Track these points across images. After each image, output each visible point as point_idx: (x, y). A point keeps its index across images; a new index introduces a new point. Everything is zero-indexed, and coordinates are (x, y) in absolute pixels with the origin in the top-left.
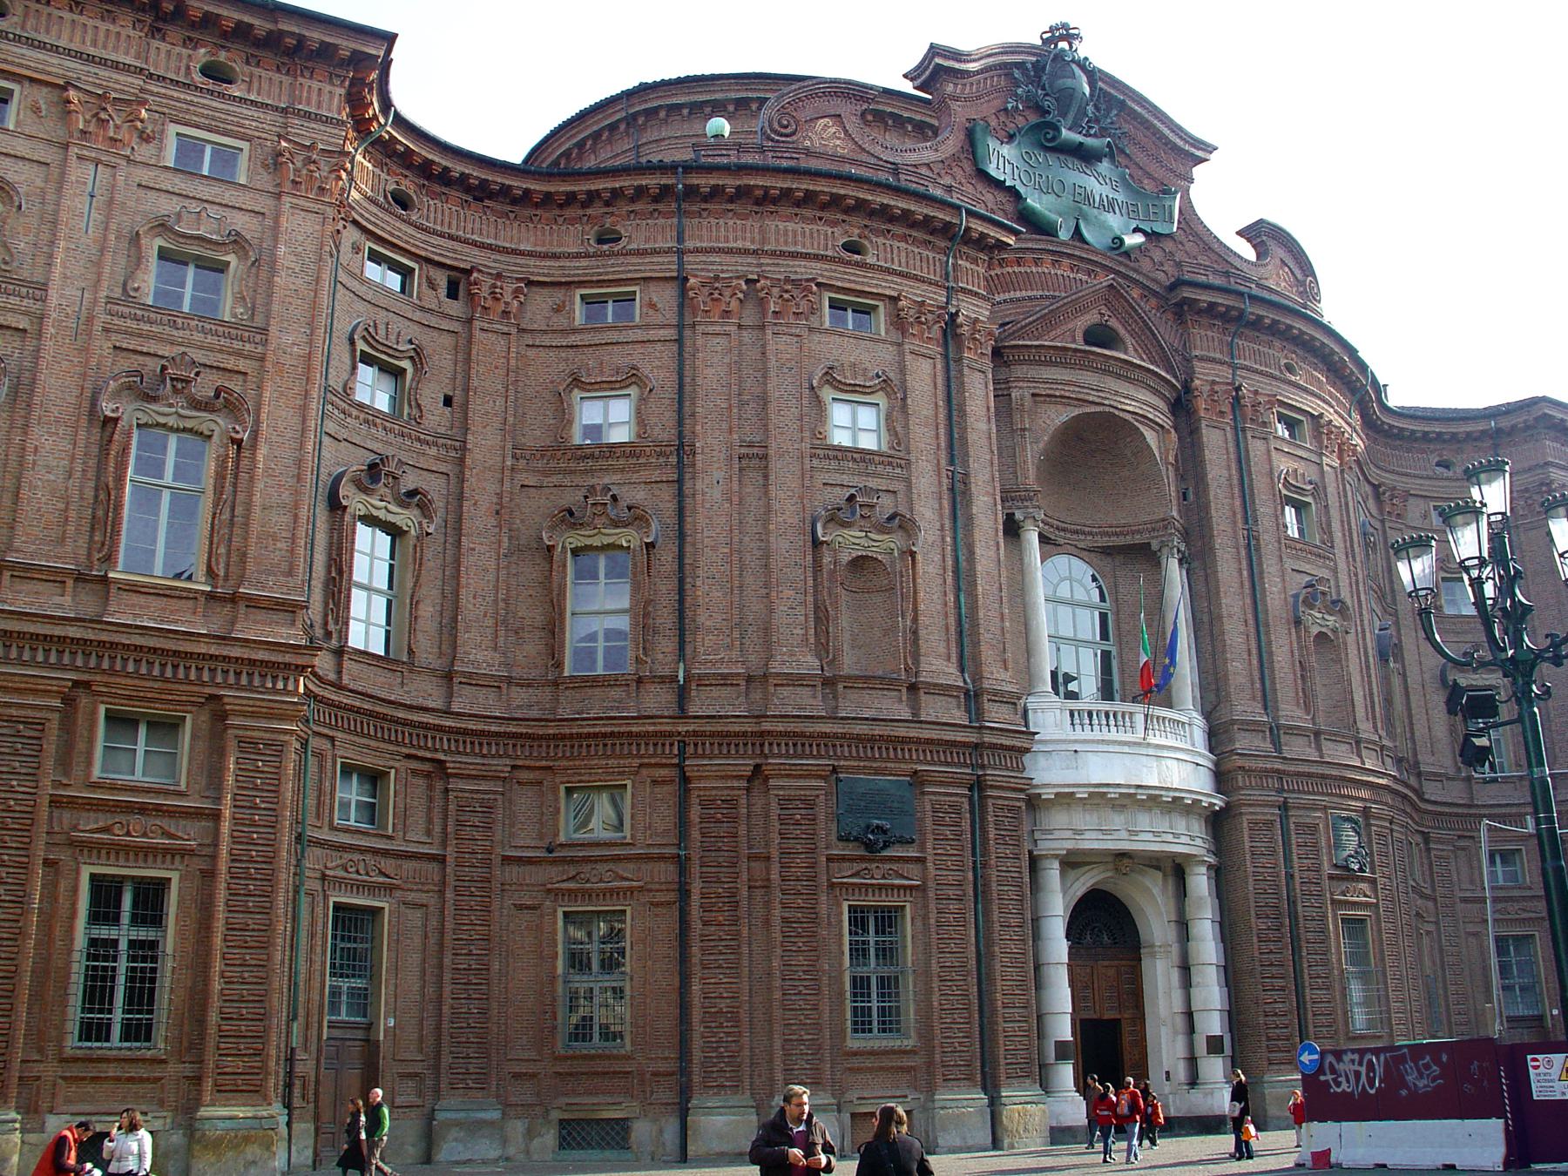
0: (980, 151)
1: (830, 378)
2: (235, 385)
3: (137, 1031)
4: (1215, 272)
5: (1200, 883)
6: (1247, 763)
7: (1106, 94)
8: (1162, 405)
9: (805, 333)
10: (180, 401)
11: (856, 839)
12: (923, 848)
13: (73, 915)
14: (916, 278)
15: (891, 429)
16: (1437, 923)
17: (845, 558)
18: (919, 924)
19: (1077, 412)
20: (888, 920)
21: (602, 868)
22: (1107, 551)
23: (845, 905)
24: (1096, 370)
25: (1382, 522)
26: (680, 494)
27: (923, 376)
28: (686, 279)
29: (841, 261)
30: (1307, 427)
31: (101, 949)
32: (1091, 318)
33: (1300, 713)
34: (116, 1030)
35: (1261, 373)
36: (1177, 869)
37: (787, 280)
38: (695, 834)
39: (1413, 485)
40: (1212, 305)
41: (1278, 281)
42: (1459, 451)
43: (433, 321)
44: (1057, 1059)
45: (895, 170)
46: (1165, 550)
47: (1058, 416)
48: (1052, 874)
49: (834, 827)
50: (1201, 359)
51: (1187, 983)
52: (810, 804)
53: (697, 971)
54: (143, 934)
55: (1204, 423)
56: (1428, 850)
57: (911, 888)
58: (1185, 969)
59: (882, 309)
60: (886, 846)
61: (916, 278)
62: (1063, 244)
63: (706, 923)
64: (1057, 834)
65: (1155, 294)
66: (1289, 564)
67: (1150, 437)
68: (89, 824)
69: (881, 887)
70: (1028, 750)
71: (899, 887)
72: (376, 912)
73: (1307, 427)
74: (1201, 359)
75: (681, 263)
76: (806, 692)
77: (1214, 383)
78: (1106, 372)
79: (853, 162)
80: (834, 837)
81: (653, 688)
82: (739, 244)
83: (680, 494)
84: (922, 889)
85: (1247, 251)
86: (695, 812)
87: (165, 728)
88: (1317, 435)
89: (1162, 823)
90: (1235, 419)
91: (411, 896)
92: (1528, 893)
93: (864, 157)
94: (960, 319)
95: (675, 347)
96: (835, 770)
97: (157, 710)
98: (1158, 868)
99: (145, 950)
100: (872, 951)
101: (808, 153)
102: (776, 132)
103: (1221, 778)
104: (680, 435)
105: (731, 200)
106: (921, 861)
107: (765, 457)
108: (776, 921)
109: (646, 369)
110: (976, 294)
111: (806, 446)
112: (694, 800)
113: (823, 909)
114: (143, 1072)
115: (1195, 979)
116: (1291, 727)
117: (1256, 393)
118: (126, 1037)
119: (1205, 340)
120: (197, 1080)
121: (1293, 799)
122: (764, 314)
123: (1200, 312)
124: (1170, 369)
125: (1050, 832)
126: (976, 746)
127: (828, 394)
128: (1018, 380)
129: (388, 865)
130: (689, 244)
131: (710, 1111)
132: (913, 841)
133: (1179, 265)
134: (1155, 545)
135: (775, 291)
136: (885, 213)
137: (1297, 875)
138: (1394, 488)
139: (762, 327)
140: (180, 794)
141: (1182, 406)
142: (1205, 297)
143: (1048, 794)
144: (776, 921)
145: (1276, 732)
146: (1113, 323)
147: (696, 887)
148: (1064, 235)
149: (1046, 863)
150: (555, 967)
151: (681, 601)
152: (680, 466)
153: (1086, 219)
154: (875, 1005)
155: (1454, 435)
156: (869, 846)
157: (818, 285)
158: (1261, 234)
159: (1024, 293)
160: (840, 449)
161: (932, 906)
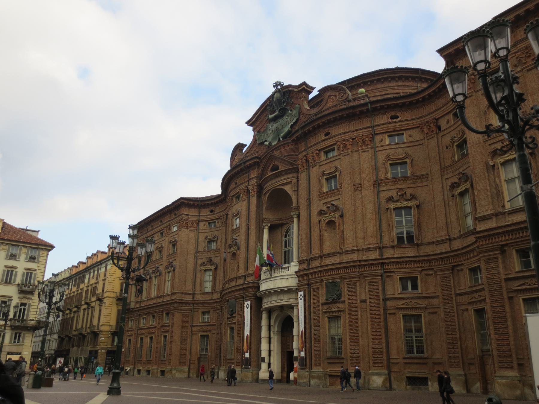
7: (286, 91)
36: (291, 307)
39: (437, 115)
40: (297, 137)
43: (218, 229)
62: (275, 145)
67: (287, 188)
91: (213, 332)
96: (228, 300)
106: (235, 317)
117: (312, 153)
126: (244, 289)
129: (208, 327)
137: (312, 304)
138: (427, 122)
154: (337, 345)
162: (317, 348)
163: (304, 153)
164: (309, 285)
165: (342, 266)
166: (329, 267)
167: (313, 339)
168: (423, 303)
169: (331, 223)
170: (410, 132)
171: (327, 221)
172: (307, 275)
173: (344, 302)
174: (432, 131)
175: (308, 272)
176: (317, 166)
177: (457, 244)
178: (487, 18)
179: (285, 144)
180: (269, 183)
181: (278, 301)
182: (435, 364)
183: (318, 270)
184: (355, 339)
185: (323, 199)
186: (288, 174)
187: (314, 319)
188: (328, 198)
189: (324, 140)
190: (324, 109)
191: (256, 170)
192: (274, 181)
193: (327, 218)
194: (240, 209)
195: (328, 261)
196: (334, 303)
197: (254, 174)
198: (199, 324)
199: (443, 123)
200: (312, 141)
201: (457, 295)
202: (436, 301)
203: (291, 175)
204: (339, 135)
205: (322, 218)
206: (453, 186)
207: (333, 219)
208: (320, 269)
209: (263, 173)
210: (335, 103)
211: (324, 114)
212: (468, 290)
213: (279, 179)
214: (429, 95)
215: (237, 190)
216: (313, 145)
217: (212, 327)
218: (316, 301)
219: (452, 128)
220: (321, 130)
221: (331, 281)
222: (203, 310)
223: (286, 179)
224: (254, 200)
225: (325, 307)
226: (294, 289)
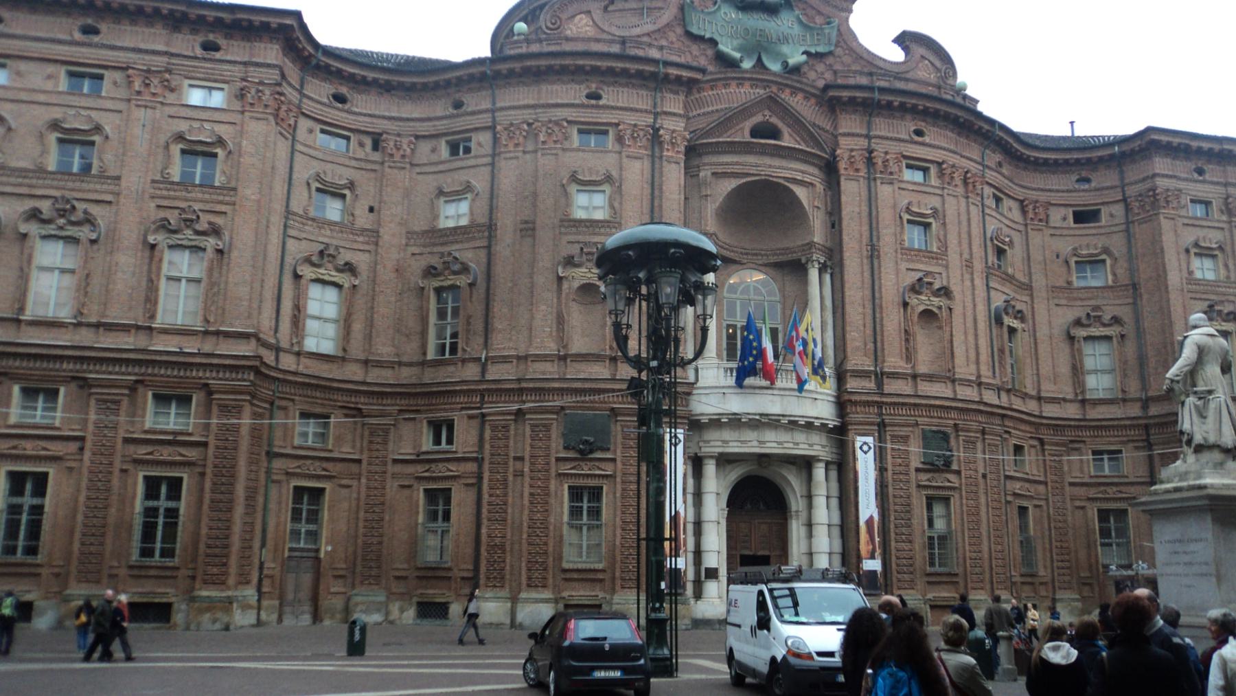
0: (687, 19)
1: (574, 178)
2: (219, 220)
3: (168, 553)
4: (861, 73)
5: (819, 472)
6: (854, 398)
8: (816, 171)
9: (560, 152)
10: (189, 232)
11: (574, 448)
12: (615, 451)
13: (134, 497)
14: (631, 110)
15: (612, 206)
16: (1047, 500)
17: (576, 284)
18: (611, 496)
19: (744, 180)
20: (596, 494)
21: (440, 465)
22: (778, 266)
23: (566, 486)
24: (756, 153)
25: (1026, 225)
26: (489, 255)
27: (635, 172)
28: (495, 127)
29: (588, 106)
30: (933, 170)
31: (151, 513)
32: (758, 119)
33: (903, 364)
34: (157, 553)
35: (891, 139)
36: (805, 464)
37: (550, 121)
38: (487, 446)
39: (1054, 198)
41: (926, 73)
42: (1095, 169)
44: (706, 577)
45: (623, 42)
46: (810, 265)
47: (730, 185)
48: (710, 468)
49: (561, 441)
50: (844, 135)
51: (810, 535)
52: (547, 428)
53: (485, 522)
54: (171, 504)
55: (842, 179)
56: (1043, 450)
57: (607, 476)
58: (810, 525)
59: (611, 133)
60: (591, 452)
61: (631, 110)
62: (746, 71)
63: (491, 496)
64: (712, 444)
65: (813, 95)
66: (904, 266)
67: (801, 192)
68: (141, 451)
69: (588, 476)
70: (689, 394)
71: (599, 476)
72: (321, 491)
73: (933, 170)
74: (844, 135)
75: (494, 118)
76: (548, 365)
77: (852, 150)
78: (763, 153)
79: (598, 40)
80: (561, 448)
81: (471, 365)
82: (526, 102)
83: (489, 255)
84: (613, 477)
85: (896, 55)
86: (488, 433)
87: (184, 400)
88: (941, 174)
89: (784, 436)
90: (869, 172)
92: (1126, 480)
93: (605, 36)
94: (662, 132)
95: (489, 168)
96: (563, 408)
97: (179, 391)
98: (793, 463)
99: (172, 513)
100: (585, 513)
101: (567, 39)
102: (547, 28)
103: (842, 404)
104: (491, 219)
105: (520, 76)
106: (614, 460)
107: (534, 229)
108: (526, 494)
109: (474, 183)
110: (674, 114)
111: (556, 221)
112: (487, 427)
113: (552, 487)
114: (168, 573)
115: (814, 533)
116: (893, 373)
117: (886, 153)
118: (162, 555)
119: (850, 123)
120: (193, 578)
121: (887, 419)
122: (536, 142)
123: (844, 104)
124: (818, 144)
125: (708, 442)
127: (573, 188)
128: (705, 164)
130: (499, 105)
131: (487, 599)
132: (608, 449)
133: (835, 72)
134: (803, 261)
135: (544, 129)
136: (611, 72)
137: (890, 467)
138: (1037, 202)
139: (535, 151)
140: (190, 434)
141: (830, 169)
142: (845, 94)
143: (705, 420)
144: (526, 494)
145: (880, 377)
146: (774, 120)
147: (486, 475)
148: (747, 64)
149: (706, 461)
150: (417, 520)
151: (487, 315)
152: (490, 238)
153: (766, 50)
155: (1089, 160)
156: (581, 452)
157: (569, 122)
158: (905, 40)
159: (715, 108)
160: (581, 221)
161: (619, 487)
162: (904, 554)
163: (864, 143)
164: (882, 426)
165: (960, 405)
166: (938, 402)
167: (893, 535)
168: (1033, 489)
169: (928, 315)
170: (1012, 203)
171: (921, 308)
172: (880, 405)
173: (958, 473)
174: (1040, 220)
175: (884, 400)
176: (896, 186)
177: (1072, 411)
178: (1220, 133)
179: (787, 86)
180: (751, 159)
181: (786, 445)
182: (1041, 584)
183: (912, 401)
184: (976, 540)
185: (908, 260)
186: (806, 162)
187: (895, 496)
188: (918, 261)
189: (916, 143)
190: (908, 76)
191: (682, 97)
192: (768, 161)
193: (921, 302)
194: (615, 173)
195: (926, 388)
196: (943, 471)
197: (673, 103)
198: (289, 451)
199: (1056, 216)
200: (882, 127)
201: (1071, 484)
202: (1041, 488)
203: (811, 169)
204: (944, 149)
205: (913, 300)
206: (1078, 323)
207: (935, 310)
208: (918, 401)
209: (728, 121)
210: (933, 78)
211: (911, 87)
212: (1087, 480)
213: (784, 163)
214: (1046, 160)
215: (605, 117)
216: (887, 138)
217: (340, 466)
218: (900, 461)
219: (1072, 232)
220: (908, 117)
221: (934, 428)
222: (307, 408)
223: (803, 172)
224: (674, 176)
225: (923, 477)
226: (831, 424)
